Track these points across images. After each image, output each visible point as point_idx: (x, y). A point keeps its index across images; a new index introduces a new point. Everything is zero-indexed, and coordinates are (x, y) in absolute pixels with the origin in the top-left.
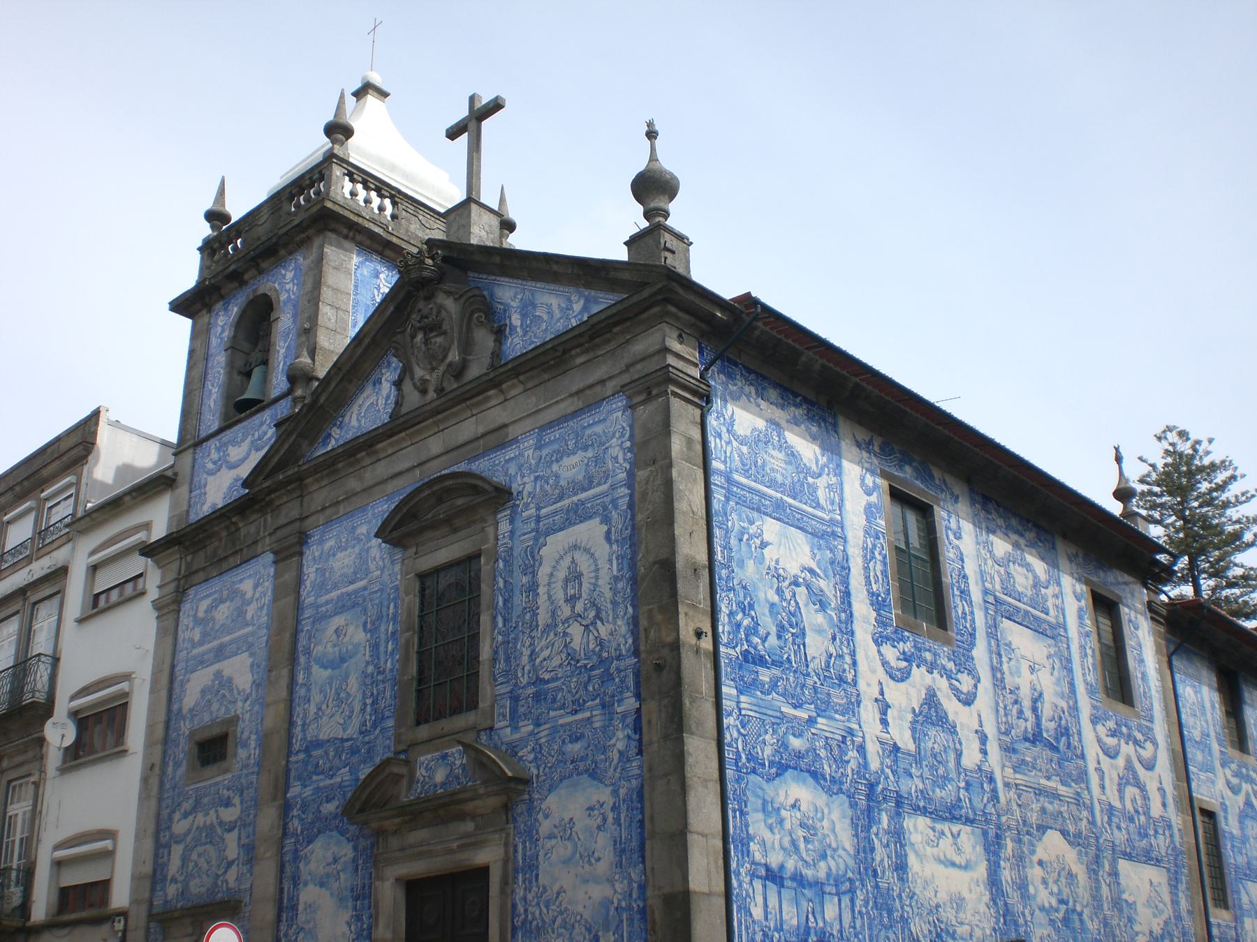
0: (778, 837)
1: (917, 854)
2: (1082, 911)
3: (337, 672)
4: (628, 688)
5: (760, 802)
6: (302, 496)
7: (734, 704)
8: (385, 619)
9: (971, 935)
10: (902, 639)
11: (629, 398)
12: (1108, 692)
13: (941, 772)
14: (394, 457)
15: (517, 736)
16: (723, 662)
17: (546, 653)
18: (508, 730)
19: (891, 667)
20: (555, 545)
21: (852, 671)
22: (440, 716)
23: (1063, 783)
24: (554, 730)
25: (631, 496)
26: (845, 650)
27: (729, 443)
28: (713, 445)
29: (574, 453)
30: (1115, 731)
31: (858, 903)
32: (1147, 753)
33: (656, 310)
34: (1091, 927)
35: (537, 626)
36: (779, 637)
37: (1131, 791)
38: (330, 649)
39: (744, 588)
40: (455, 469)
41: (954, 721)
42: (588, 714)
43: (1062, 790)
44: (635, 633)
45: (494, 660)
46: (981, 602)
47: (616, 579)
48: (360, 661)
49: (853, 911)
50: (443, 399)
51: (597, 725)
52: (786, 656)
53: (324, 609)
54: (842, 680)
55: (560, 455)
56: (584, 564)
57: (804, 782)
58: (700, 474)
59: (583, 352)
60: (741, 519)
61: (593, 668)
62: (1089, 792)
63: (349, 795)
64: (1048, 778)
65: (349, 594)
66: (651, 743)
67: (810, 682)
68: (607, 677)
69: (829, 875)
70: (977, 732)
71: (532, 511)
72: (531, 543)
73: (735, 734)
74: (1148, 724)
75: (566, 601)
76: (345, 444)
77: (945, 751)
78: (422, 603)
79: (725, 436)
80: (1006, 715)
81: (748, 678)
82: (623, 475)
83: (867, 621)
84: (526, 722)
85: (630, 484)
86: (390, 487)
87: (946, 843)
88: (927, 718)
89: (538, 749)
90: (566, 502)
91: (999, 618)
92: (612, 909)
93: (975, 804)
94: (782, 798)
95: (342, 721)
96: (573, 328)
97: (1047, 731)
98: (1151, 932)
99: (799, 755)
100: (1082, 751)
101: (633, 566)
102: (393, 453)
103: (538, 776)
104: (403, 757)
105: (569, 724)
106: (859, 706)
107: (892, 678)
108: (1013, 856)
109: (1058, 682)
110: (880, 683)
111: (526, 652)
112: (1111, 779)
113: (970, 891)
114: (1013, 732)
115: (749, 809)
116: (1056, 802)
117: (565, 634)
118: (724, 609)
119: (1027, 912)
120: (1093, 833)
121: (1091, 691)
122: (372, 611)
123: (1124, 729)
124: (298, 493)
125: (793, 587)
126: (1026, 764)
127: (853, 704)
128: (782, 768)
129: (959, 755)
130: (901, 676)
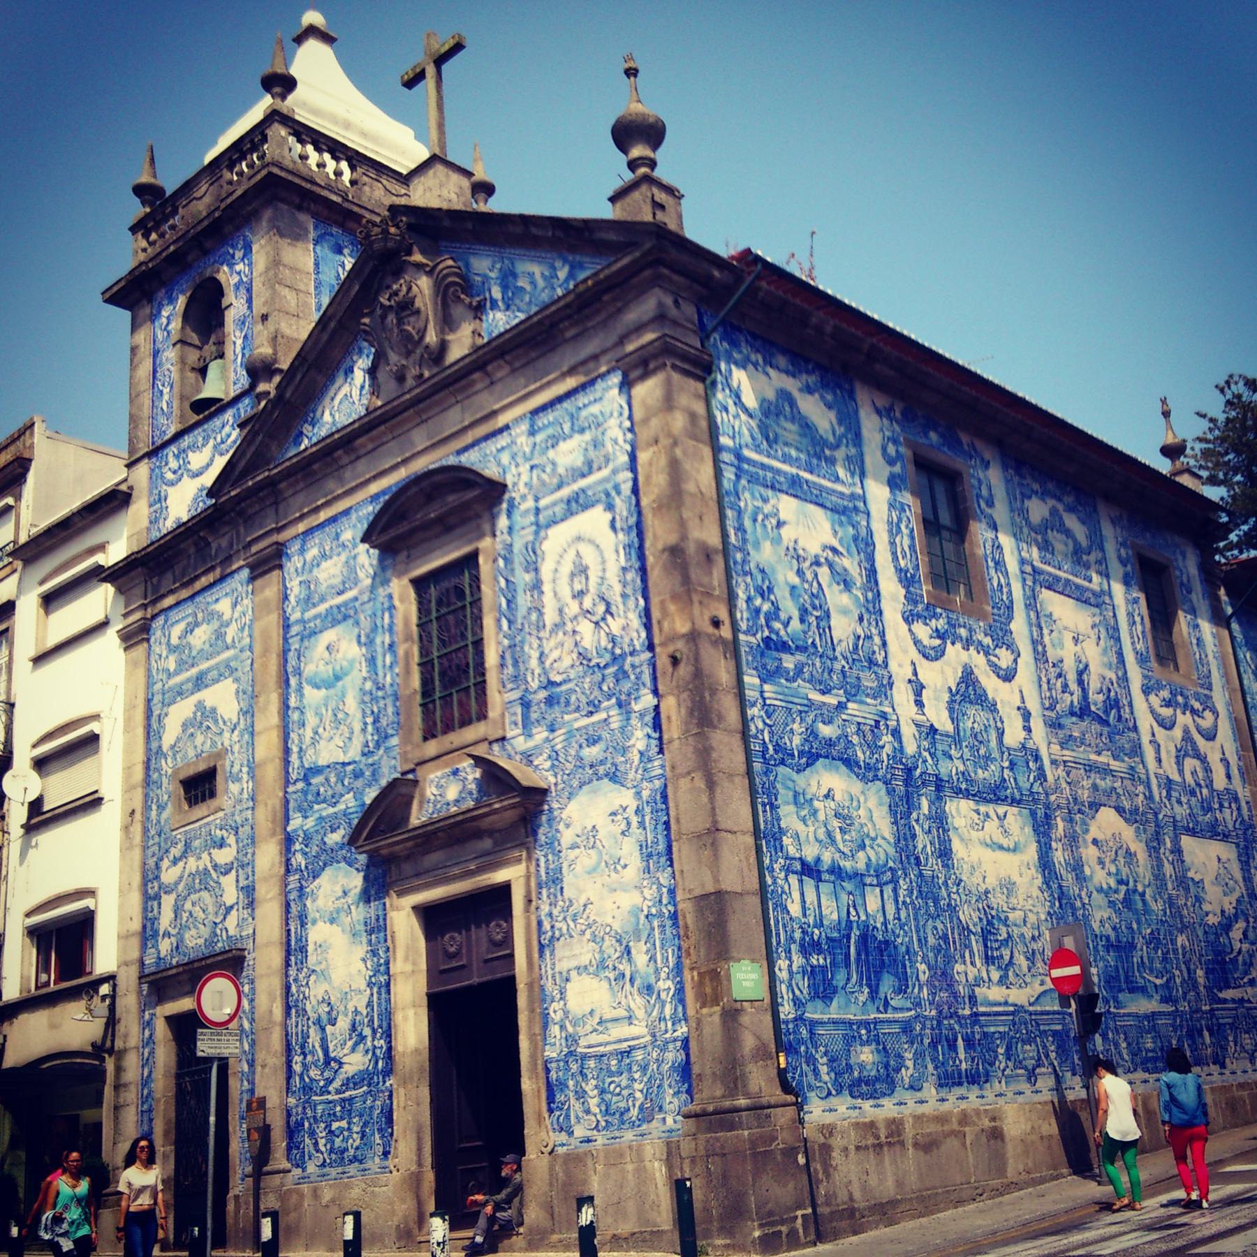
0: (812, 829)
1: (962, 840)
3: (332, 691)
4: (644, 684)
5: (791, 794)
6: (276, 503)
7: (757, 694)
8: (380, 630)
9: (1025, 921)
10: (935, 616)
11: (625, 375)
12: (1161, 660)
13: (982, 752)
14: (375, 454)
15: (531, 744)
16: (744, 649)
17: (555, 654)
18: (522, 738)
20: (557, 538)
21: (883, 653)
22: (448, 728)
23: (1115, 758)
24: (570, 735)
25: (635, 480)
26: (874, 631)
27: (737, 416)
28: (719, 420)
29: (571, 437)
31: (902, 893)
32: (1207, 721)
33: (647, 273)
34: (1153, 906)
35: (544, 626)
36: (802, 621)
37: (1190, 763)
38: (322, 668)
39: (763, 571)
40: (444, 463)
42: (603, 715)
43: (1115, 765)
44: (648, 626)
45: (502, 666)
47: (624, 569)
48: (357, 676)
49: (897, 901)
50: (424, 386)
51: (614, 726)
52: (810, 641)
53: (312, 625)
54: (872, 662)
55: (554, 441)
56: (590, 557)
57: (837, 769)
58: (707, 452)
59: (571, 325)
60: (753, 497)
61: (606, 666)
62: (1144, 766)
63: (355, 822)
64: (1099, 754)
65: (338, 607)
66: (670, 742)
67: (837, 666)
68: (621, 675)
69: (868, 866)
70: (1019, 708)
71: (530, 503)
72: (531, 538)
73: (761, 726)
74: (1206, 692)
75: (574, 597)
76: (319, 442)
78: (420, 610)
79: (732, 409)
80: (1049, 689)
81: (771, 665)
82: (624, 459)
83: (894, 598)
84: (540, 729)
85: (633, 467)
86: (374, 488)
87: (992, 826)
88: (965, 698)
89: (555, 756)
90: (566, 492)
92: (642, 918)
93: (1021, 784)
94: (813, 789)
95: (341, 744)
96: (560, 298)
97: (1095, 704)
98: (1223, 912)
99: (830, 743)
101: (642, 557)
102: (374, 449)
103: (556, 784)
104: (410, 776)
105: (585, 727)
106: (891, 685)
107: (924, 656)
109: (1105, 651)
110: (913, 664)
111: (535, 655)
112: (1168, 752)
114: (1058, 707)
115: (779, 801)
116: (1109, 778)
117: (574, 632)
118: (742, 595)
119: (1083, 894)
121: (1142, 660)
122: (366, 624)
123: (1180, 699)
124: (272, 500)
125: (815, 567)
127: (884, 686)
128: (811, 758)
129: (1001, 734)
130: (938, 654)
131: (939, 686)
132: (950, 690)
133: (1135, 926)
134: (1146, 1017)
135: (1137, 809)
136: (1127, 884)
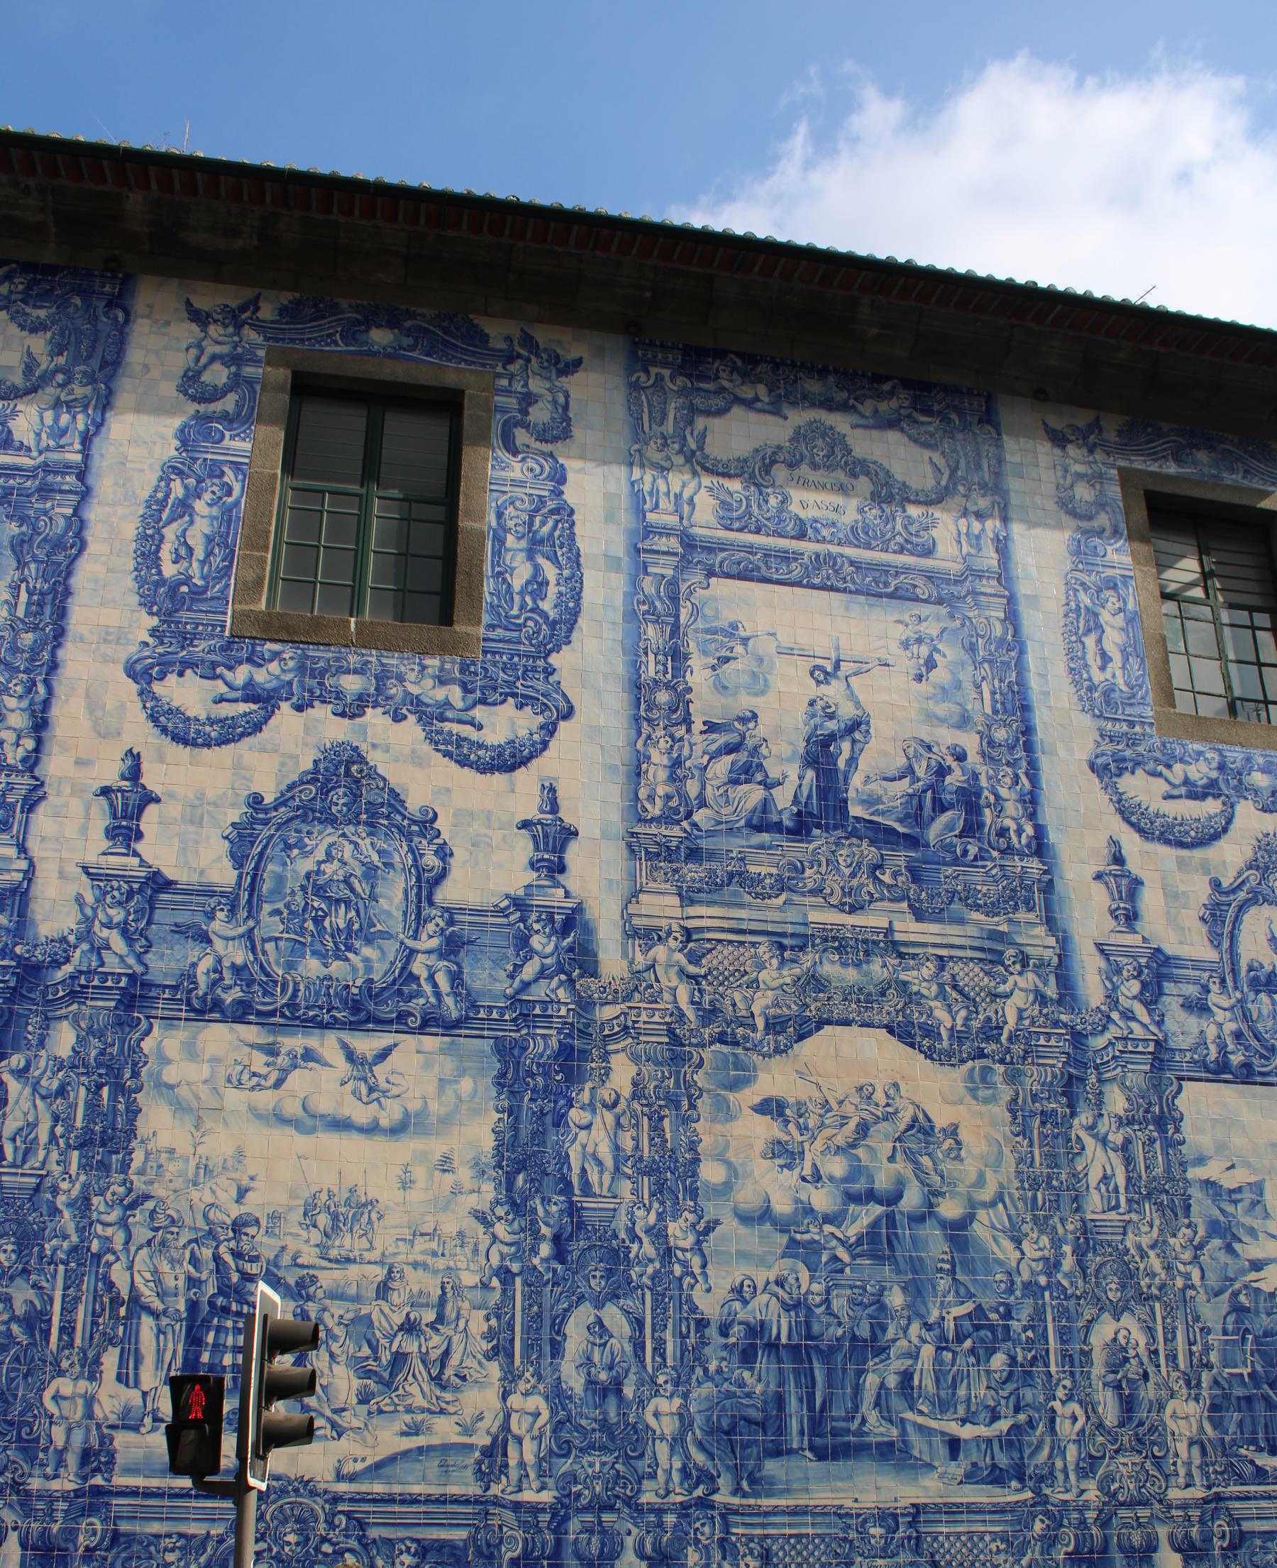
2: (969, 1218)
9: (383, 1290)
19: (188, 719)
23: (919, 915)
30: (1213, 783)
41: (424, 810)
43: (908, 928)
46: (619, 548)
70: (525, 825)
77: (370, 873)
80: (672, 778)
91: (697, 577)
100: (1040, 832)
107: (180, 739)
108: (635, 1096)
109: (944, 693)
112: (1171, 895)
113: (406, 1185)
114: (700, 816)
119: (673, 1228)
120: (1056, 1024)
126: (759, 879)
130: (229, 733)
131: (211, 794)
132: (256, 801)
133: (896, 1299)
134: (888, 1518)
135: (991, 1031)
136: (894, 1198)
